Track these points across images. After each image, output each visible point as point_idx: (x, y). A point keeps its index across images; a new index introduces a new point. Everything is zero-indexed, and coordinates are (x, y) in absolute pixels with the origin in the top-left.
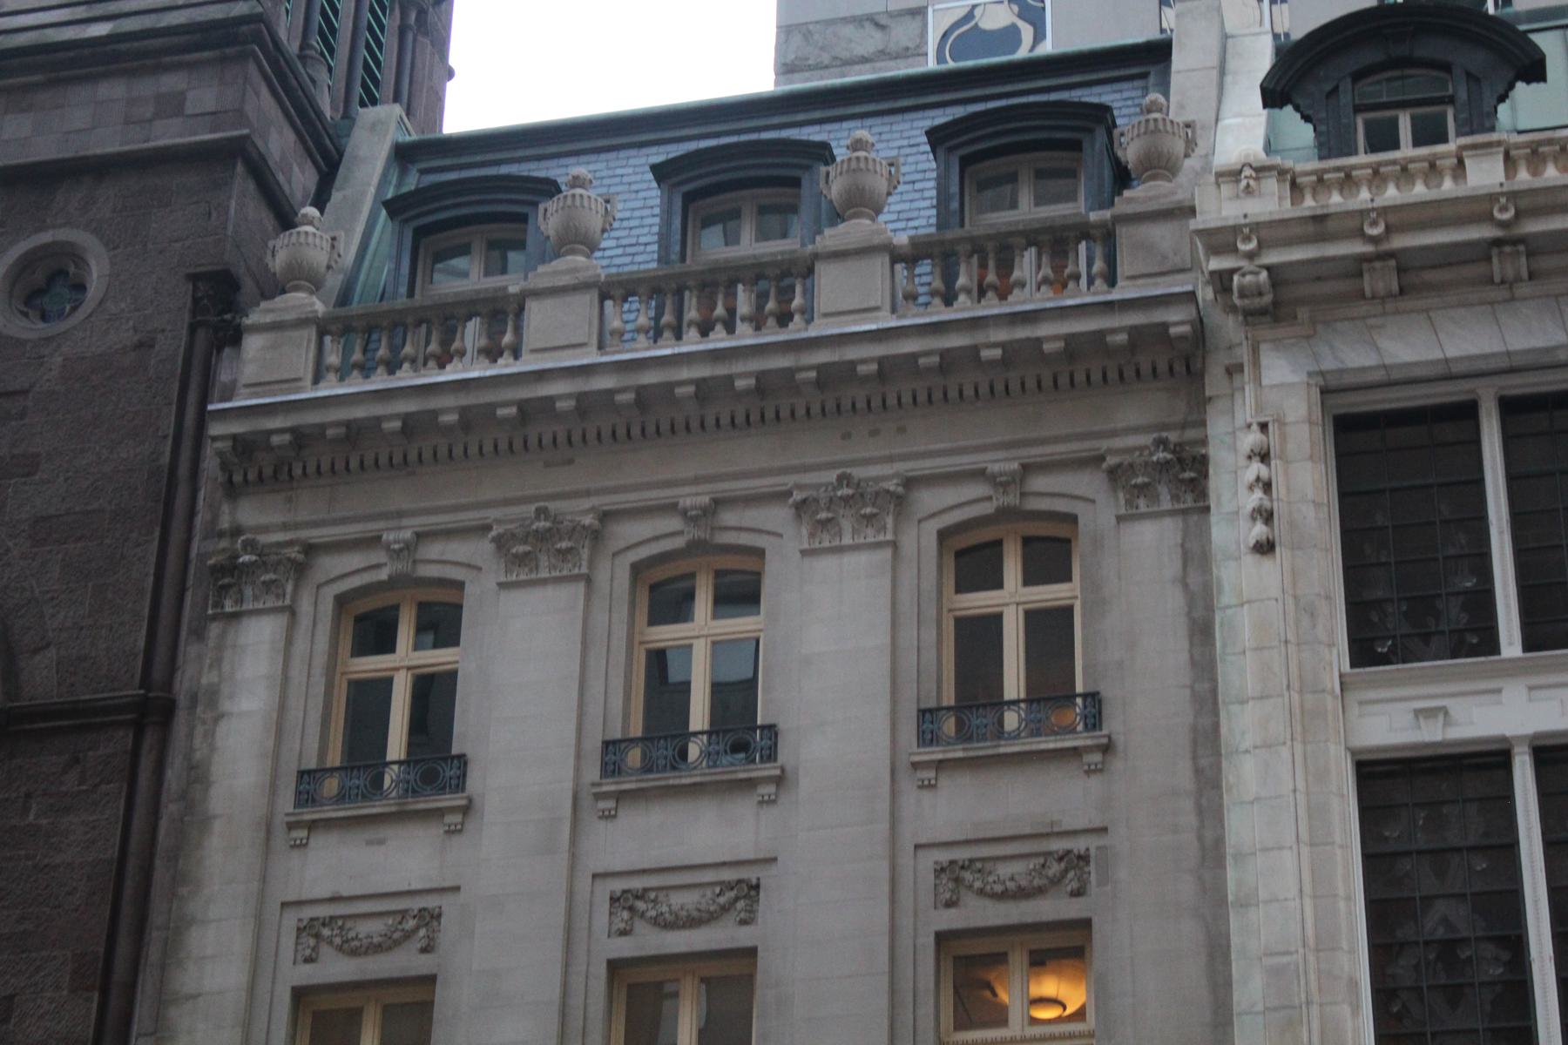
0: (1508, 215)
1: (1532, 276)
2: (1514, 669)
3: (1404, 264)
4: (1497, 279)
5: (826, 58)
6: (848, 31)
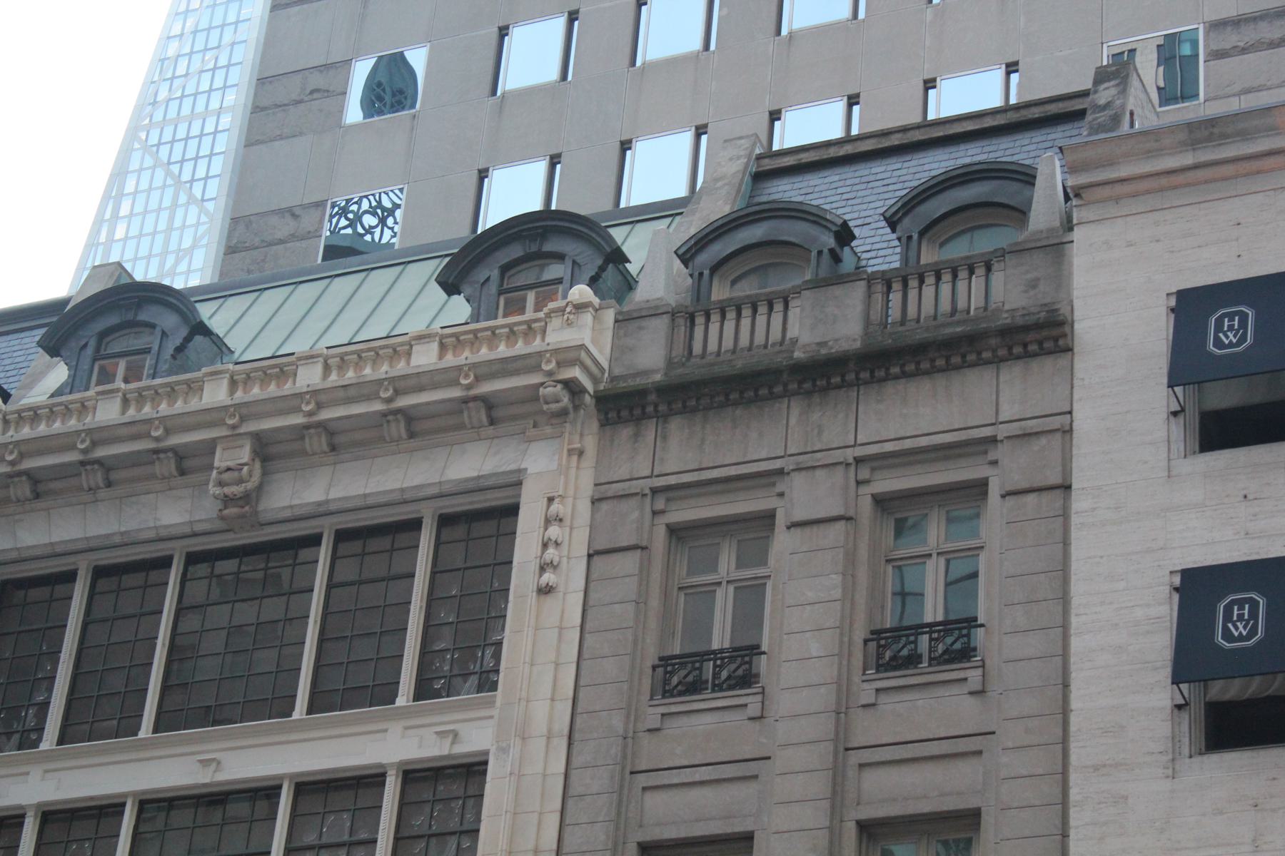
0: (552, 366)
1: (109, 484)
2: (404, 713)
3: (33, 478)
4: (85, 486)
5: (257, 241)
6: (274, 220)
